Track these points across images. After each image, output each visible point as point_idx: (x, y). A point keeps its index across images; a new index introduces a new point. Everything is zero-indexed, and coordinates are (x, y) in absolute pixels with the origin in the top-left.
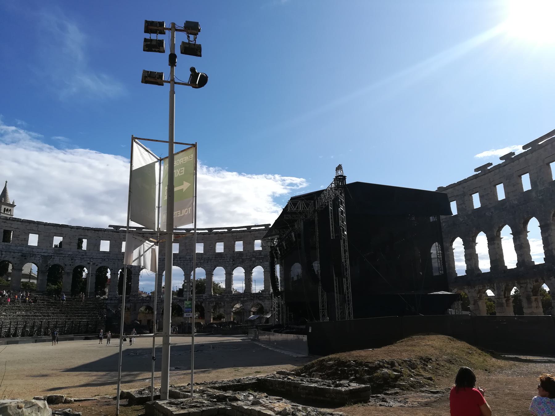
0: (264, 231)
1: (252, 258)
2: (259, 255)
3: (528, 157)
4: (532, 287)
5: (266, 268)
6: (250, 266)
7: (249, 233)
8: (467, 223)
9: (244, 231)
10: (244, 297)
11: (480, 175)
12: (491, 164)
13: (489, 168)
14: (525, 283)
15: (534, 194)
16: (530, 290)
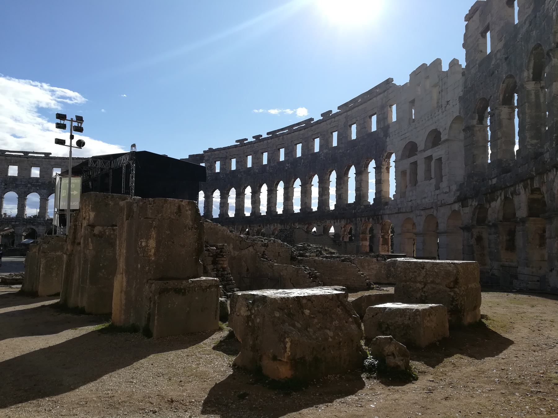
0: (44, 159)
1: (28, 184)
2: (35, 182)
3: (269, 141)
4: (257, 230)
5: (43, 196)
6: (25, 192)
7: (26, 159)
8: (225, 180)
9: (20, 156)
10: (15, 222)
11: (238, 146)
12: (247, 140)
13: (245, 142)
14: (253, 227)
15: (268, 168)
16: (255, 232)
